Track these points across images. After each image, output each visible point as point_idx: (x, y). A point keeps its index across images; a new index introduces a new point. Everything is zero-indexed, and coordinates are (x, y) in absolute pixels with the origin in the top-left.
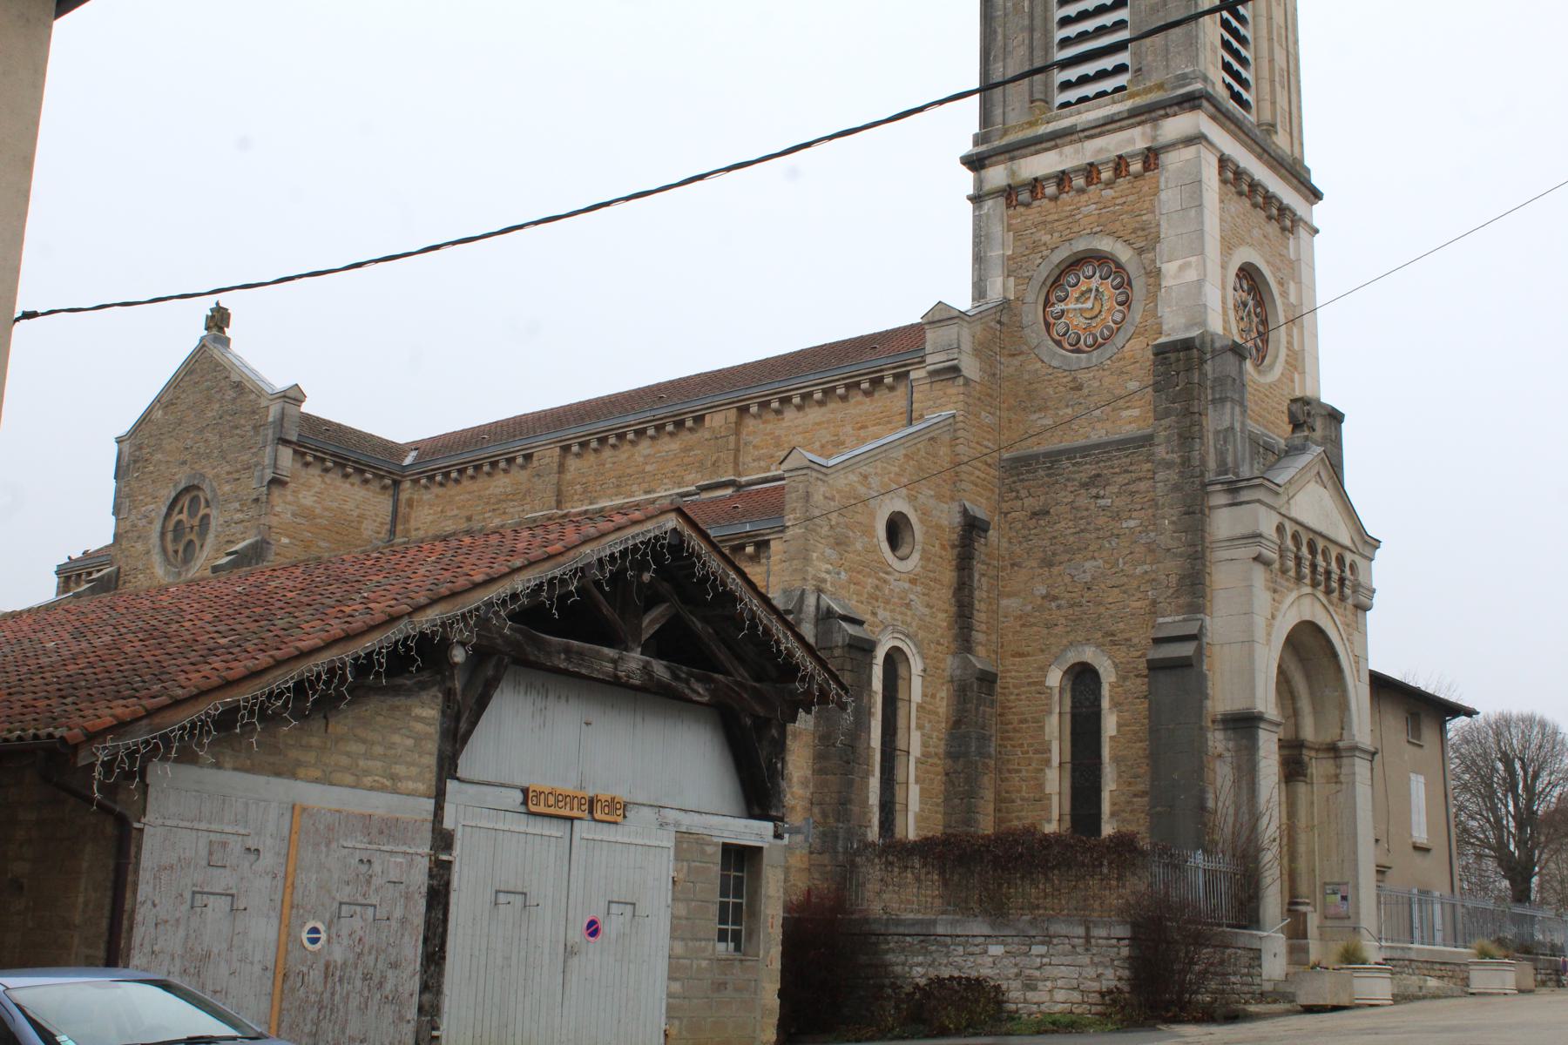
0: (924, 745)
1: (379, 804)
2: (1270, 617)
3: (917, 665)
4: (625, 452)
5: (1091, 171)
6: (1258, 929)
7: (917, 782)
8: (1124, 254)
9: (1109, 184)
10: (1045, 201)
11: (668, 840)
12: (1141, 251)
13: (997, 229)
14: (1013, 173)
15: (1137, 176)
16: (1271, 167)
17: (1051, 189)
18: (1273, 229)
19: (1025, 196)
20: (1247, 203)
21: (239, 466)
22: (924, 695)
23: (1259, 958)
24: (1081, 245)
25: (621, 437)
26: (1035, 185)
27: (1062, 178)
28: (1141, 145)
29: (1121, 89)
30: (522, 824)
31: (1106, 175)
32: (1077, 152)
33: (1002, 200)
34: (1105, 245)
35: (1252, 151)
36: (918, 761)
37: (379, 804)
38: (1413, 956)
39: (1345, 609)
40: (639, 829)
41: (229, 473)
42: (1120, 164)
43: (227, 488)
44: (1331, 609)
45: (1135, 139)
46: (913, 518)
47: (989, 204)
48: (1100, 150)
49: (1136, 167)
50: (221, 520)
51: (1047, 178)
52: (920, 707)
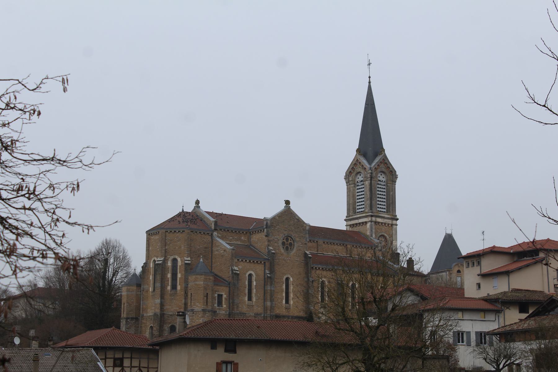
4: (333, 246)
5: (385, 224)
8: (388, 237)
9: (386, 226)
10: (378, 225)
12: (389, 238)
13: (374, 227)
14: (376, 220)
15: (390, 227)
17: (380, 224)
19: (377, 224)
21: (300, 236)
24: (383, 234)
25: (334, 244)
26: (379, 223)
27: (382, 223)
28: (390, 223)
29: (385, 212)
31: (387, 225)
32: (383, 220)
33: (374, 223)
34: (386, 235)
41: (298, 236)
42: (388, 224)
43: (298, 239)
45: (390, 222)
47: (373, 223)
48: (386, 221)
49: (390, 226)
50: (297, 245)
51: (380, 222)
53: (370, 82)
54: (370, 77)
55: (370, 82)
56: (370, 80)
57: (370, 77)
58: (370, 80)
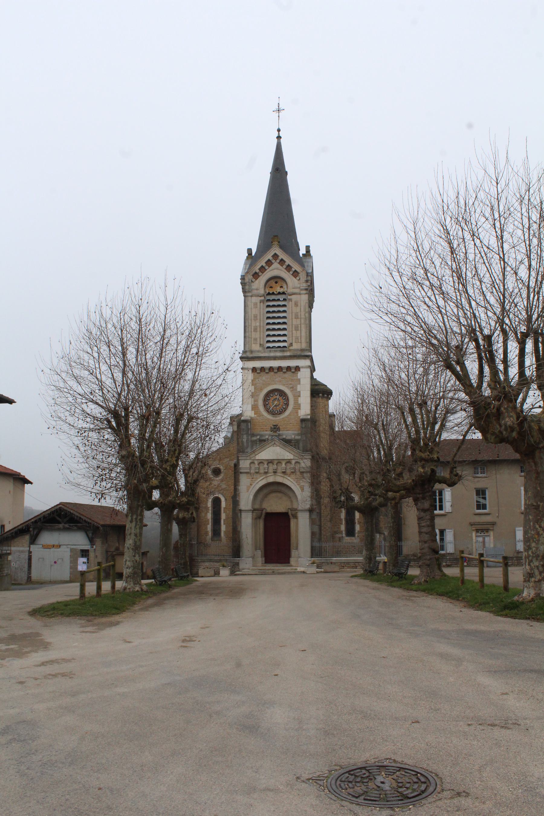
0: (226, 516)
1: (21, 549)
2: (249, 485)
3: (223, 499)
6: (239, 557)
7: (224, 524)
11: (69, 550)
16: (282, 359)
18: (289, 375)
20: (272, 373)
22: (226, 505)
23: (239, 564)
30: (43, 550)
35: (271, 360)
36: (224, 520)
37: (21, 549)
38: (333, 561)
39: (296, 474)
40: (63, 548)
44: (286, 476)
46: (221, 467)
52: (224, 508)
53: (279, 137)
54: (279, 130)
55: (279, 137)
56: (279, 134)
57: (279, 130)
58: (279, 134)
